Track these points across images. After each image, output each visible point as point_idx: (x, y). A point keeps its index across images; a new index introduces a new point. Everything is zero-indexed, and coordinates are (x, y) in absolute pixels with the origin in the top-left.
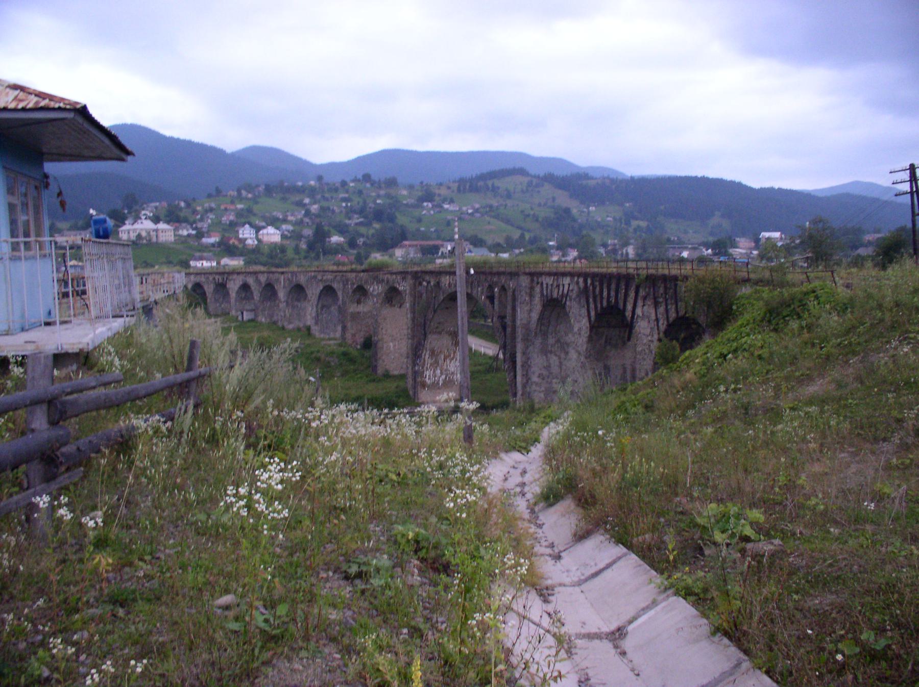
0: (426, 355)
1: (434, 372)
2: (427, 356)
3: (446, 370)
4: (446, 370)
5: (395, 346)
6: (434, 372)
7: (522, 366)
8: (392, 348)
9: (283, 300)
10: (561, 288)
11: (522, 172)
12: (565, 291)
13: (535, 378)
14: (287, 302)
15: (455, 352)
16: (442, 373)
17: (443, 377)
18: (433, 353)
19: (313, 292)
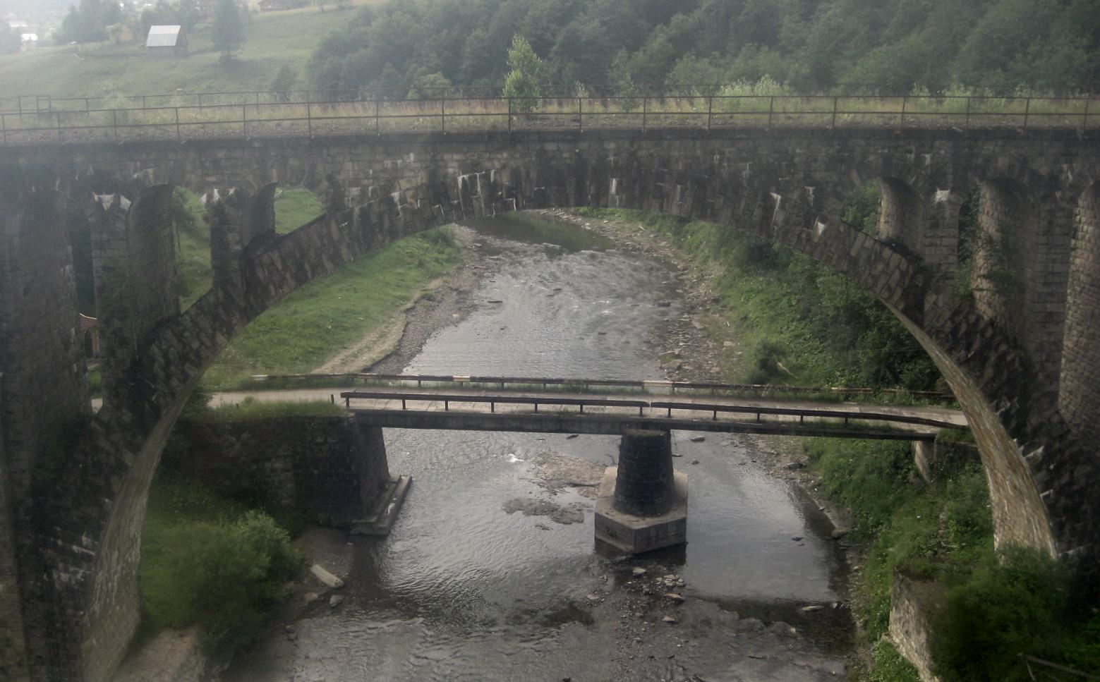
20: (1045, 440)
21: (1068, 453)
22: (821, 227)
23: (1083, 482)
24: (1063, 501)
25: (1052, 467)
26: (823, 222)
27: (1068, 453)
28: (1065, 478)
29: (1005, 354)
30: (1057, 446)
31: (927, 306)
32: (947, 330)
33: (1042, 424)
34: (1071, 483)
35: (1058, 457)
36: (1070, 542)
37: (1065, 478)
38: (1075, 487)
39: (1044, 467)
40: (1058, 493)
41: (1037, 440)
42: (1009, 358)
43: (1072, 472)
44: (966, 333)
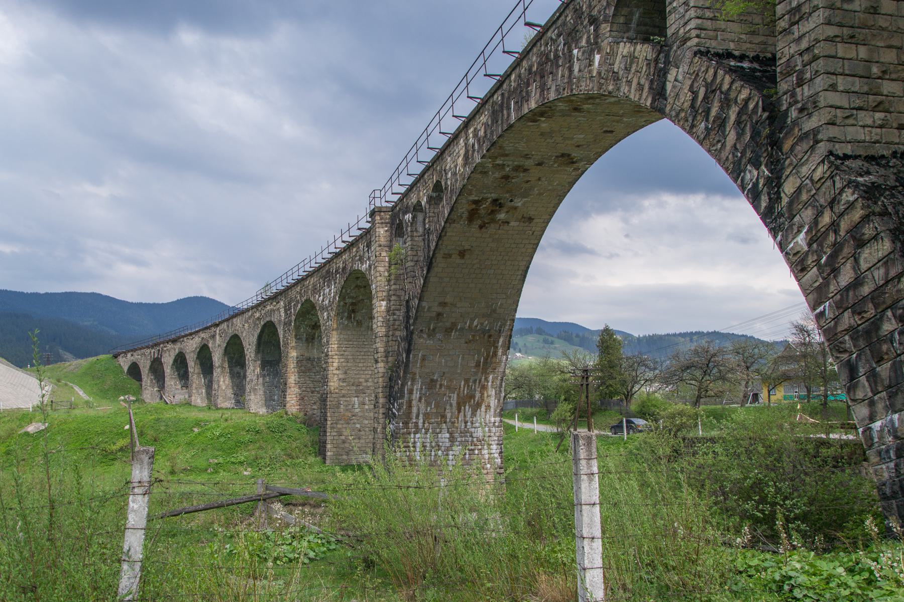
2: (416, 395)
15: (484, 388)
16: (452, 439)
20: (808, 215)
21: (844, 225)
22: (597, 57)
23: (879, 274)
24: (847, 319)
25: (823, 261)
26: (599, 53)
27: (844, 225)
28: (846, 277)
29: (747, 101)
30: (826, 219)
31: (669, 86)
32: (687, 105)
33: (799, 190)
34: (857, 283)
35: (832, 237)
36: (872, 404)
37: (846, 277)
38: (866, 290)
39: (810, 260)
40: (841, 306)
41: (797, 219)
42: (751, 106)
43: (856, 261)
44: (706, 98)
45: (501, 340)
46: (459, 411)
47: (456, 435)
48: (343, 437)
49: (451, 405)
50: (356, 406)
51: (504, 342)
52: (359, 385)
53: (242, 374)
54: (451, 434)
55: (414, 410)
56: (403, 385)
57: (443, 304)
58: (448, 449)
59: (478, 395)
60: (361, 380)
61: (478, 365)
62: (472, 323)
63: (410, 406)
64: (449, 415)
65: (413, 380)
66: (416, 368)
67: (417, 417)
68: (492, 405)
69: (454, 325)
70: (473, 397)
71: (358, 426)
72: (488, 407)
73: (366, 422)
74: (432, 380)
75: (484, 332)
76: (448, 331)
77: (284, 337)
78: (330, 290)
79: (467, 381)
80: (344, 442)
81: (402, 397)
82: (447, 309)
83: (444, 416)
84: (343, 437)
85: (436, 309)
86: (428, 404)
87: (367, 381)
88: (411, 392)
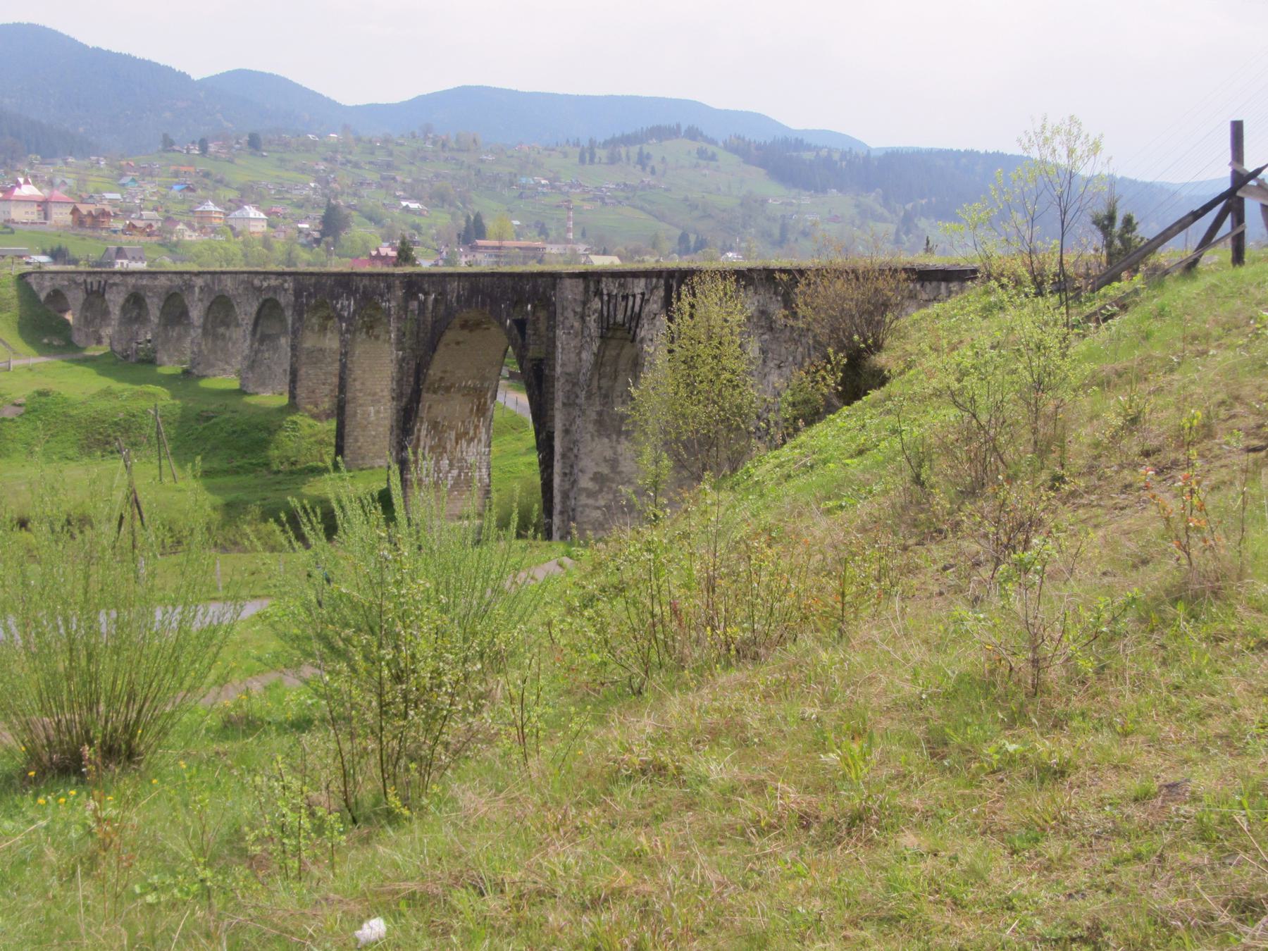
0: (422, 429)
1: (437, 462)
2: (424, 433)
3: (460, 460)
4: (460, 460)
5: (378, 412)
6: (437, 462)
7: (564, 456)
8: (373, 418)
9: (197, 324)
10: (630, 303)
11: (693, 134)
12: (637, 309)
13: (585, 482)
14: (204, 327)
15: (477, 427)
16: (451, 465)
17: (455, 472)
18: (435, 425)
19: (246, 310)
45: (489, 395)
46: (457, 443)
47: (455, 462)
48: (359, 444)
49: (451, 440)
50: (372, 415)
51: (492, 396)
52: (375, 394)
53: (227, 335)
54: (451, 461)
55: (422, 443)
56: (413, 426)
57: (445, 372)
58: (449, 472)
59: (471, 432)
60: (378, 390)
61: (472, 410)
62: (467, 382)
63: (418, 439)
64: (448, 447)
65: (422, 422)
66: (423, 413)
67: (424, 448)
68: (483, 439)
69: (452, 385)
70: (468, 433)
71: (373, 433)
72: (480, 441)
73: (381, 429)
74: (436, 422)
75: (475, 389)
76: (448, 389)
77: (293, 324)
78: (349, 305)
79: (463, 422)
80: (360, 448)
81: (413, 434)
82: (448, 375)
83: (444, 448)
84: (359, 444)
85: (439, 374)
86: (433, 438)
87: (382, 391)
88: (419, 430)
